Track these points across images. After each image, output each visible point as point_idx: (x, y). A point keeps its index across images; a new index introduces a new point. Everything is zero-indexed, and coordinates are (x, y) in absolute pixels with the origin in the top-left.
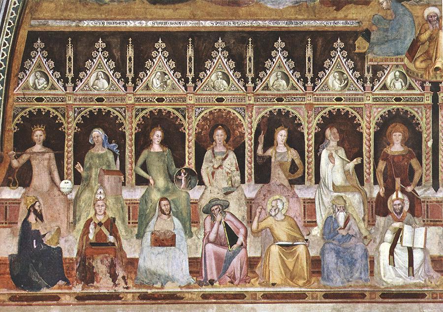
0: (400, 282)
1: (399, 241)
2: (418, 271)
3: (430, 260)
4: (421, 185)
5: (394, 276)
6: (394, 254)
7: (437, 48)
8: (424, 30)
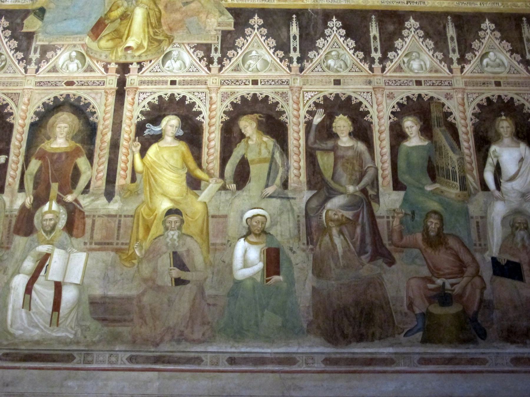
0: (36, 333)
1: (42, 273)
2: (67, 319)
3: (87, 302)
4: (87, 193)
5: (26, 325)
6: (33, 293)
7: (130, 26)
8: (116, 7)
